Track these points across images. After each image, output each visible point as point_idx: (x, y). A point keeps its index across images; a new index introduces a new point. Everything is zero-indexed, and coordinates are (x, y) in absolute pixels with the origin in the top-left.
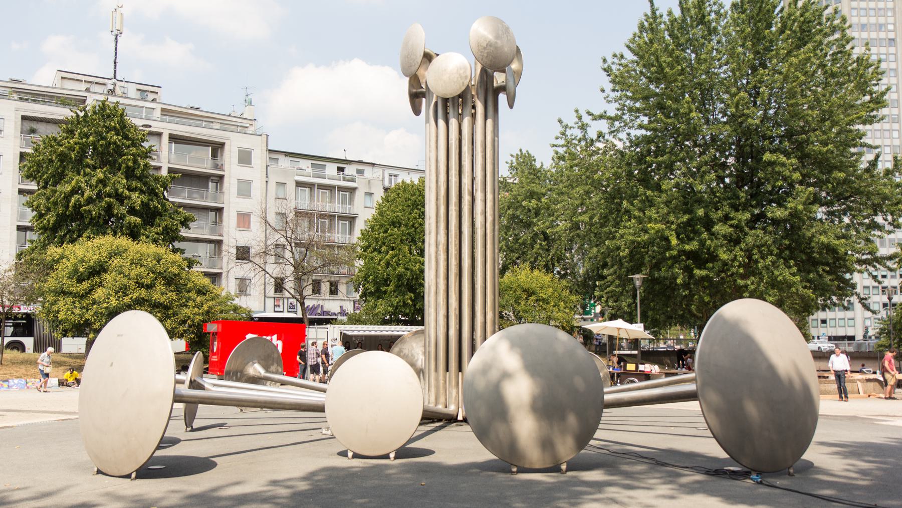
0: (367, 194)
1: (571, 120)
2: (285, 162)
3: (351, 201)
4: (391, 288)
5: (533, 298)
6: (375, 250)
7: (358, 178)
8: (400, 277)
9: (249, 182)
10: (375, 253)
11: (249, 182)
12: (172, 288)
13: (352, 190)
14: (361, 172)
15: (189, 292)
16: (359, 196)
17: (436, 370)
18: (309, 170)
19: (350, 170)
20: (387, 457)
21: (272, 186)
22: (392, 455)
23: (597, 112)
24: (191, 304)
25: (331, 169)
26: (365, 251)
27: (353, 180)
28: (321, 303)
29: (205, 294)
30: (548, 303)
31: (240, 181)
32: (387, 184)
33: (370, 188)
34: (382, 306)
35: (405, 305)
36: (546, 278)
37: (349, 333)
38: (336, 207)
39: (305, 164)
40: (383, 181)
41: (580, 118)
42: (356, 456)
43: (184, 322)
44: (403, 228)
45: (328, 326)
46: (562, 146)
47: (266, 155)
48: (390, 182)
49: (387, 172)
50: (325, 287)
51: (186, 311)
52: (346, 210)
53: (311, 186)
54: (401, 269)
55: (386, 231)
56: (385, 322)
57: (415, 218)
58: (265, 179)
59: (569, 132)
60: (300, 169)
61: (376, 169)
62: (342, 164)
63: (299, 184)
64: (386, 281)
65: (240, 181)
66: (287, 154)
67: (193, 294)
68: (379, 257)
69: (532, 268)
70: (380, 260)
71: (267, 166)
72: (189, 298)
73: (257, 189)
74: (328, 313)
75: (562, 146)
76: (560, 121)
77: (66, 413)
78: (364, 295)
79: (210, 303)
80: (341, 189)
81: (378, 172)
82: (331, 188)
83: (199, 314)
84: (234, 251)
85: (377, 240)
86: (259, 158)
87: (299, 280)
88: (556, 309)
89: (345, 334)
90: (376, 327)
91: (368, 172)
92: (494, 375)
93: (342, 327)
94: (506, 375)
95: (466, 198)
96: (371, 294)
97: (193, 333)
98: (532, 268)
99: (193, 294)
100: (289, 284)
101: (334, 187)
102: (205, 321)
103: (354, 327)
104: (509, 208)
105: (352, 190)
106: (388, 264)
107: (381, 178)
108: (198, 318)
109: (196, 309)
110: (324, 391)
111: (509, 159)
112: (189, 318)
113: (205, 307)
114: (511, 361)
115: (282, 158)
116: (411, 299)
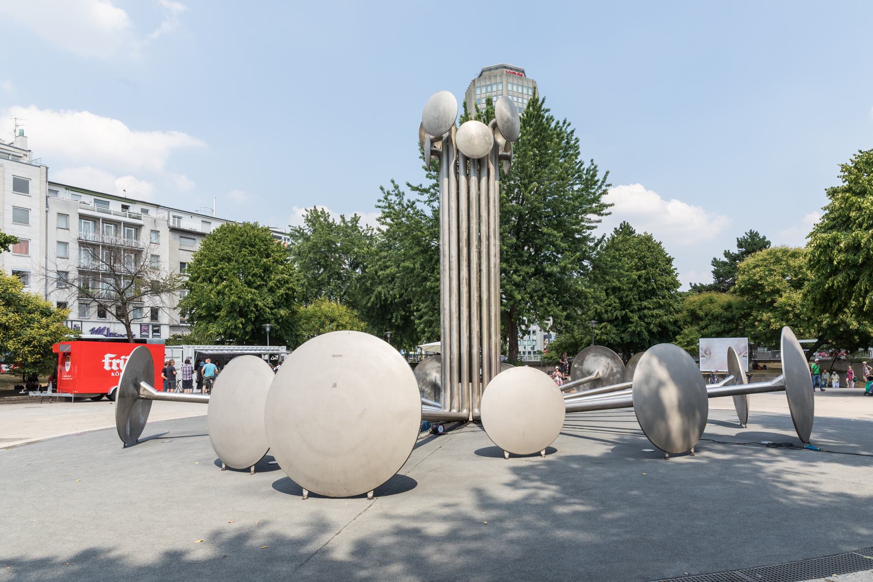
0: (152, 231)
1: (390, 187)
2: (64, 195)
3: (137, 237)
4: (222, 313)
6: (204, 280)
7: (143, 215)
8: (233, 304)
9: (26, 211)
11: (26, 211)
12: (11, 309)
13: (138, 227)
14: (145, 211)
16: (145, 233)
17: (460, 381)
18: (92, 205)
19: (135, 209)
20: (538, 454)
21: (53, 216)
22: (543, 453)
23: (415, 185)
24: (36, 325)
25: (115, 207)
27: (139, 218)
28: (108, 326)
31: (15, 208)
32: (171, 224)
33: (156, 226)
34: (213, 329)
35: (236, 328)
37: (204, 352)
38: (121, 239)
39: (89, 199)
40: (168, 221)
41: (397, 187)
42: (512, 456)
43: (28, 343)
44: (233, 263)
45: (184, 346)
46: (385, 207)
47: (45, 187)
48: (174, 222)
49: (172, 214)
51: (28, 333)
52: (133, 243)
53: (95, 219)
54: (233, 298)
55: (216, 265)
56: (222, 343)
57: (245, 256)
58: (44, 209)
59: (389, 197)
60: (84, 203)
61: (160, 211)
62: (126, 203)
63: (82, 217)
64: (219, 308)
65: (15, 208)
66: (68, 188)
67: (36, 316)
68: (210, 287)
70: (212, 290)
71: (47, 197)
72: (33, 319)
73: (36, 216)
74: (114, 334)
75: (385, 207)
76: (382, 189)
77: (15, 440)
78: (191, 320)
80: (127, 224)
81: (163, 214)
82: (117, 223)
83: (46, 335)
84: (55, 275)
85: (207, 272)
86: (37, 187)
91: (153, 212)
92: (653, 384)
93: (197, 347)
94: (661, 384)
95: (474, 243)
96: (200, 318)
99: (36, 316)
101: (119, 222)
103: (207, 347)
104: (310, 252)
105: (138, 227)
106: (219, 293)
107: (166, 218)
108: (45, 339)
110: (206, 402)
111: (305, 213)
112: (34, 338)
114: (662, 373)
115: (62, 191)
116: (241, 323)
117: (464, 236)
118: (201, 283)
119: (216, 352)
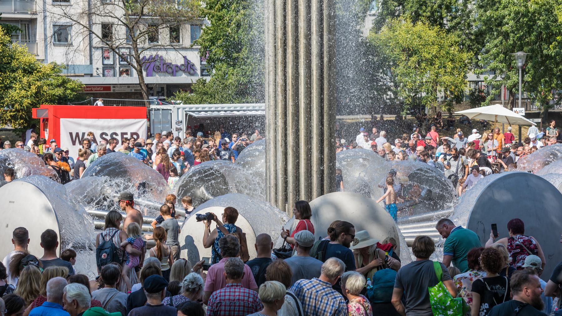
5: (414, 59)
10: (224, 11)
15: (13, 71)
26: (211, 8)
29: (31, 73)
30: (432, 64)
36: (431, 33)
37: (195, 115)
50: (164, 35)
69: (416, 18)
72: (15, 79)
79: (39, 84)
83: (27, 97)
87: (130, 30)
88: (442, 71)
89: (190, 116)
90: (226, 106)
97: (21, 118)
98: (416, 18)
100: (120, 33)
102: (34, 105)
103: (200, 106)
108: (26, 102)
109: (23, 92)
113: (34, 89)
117: (280, 35)
118: (219, 10)
119: (222, 114)
